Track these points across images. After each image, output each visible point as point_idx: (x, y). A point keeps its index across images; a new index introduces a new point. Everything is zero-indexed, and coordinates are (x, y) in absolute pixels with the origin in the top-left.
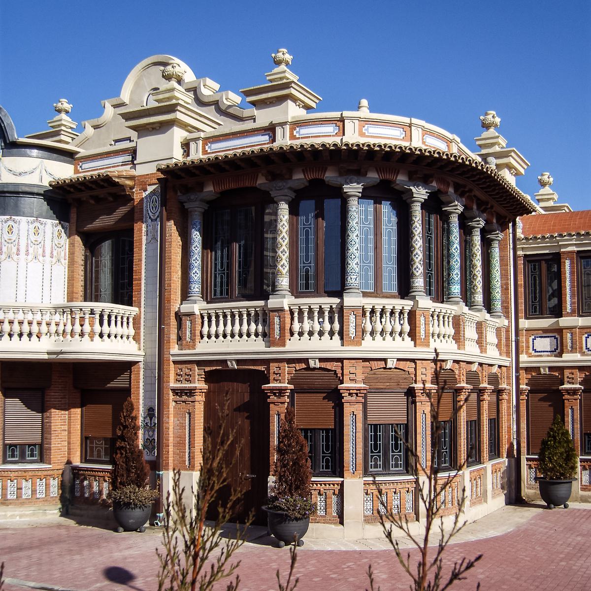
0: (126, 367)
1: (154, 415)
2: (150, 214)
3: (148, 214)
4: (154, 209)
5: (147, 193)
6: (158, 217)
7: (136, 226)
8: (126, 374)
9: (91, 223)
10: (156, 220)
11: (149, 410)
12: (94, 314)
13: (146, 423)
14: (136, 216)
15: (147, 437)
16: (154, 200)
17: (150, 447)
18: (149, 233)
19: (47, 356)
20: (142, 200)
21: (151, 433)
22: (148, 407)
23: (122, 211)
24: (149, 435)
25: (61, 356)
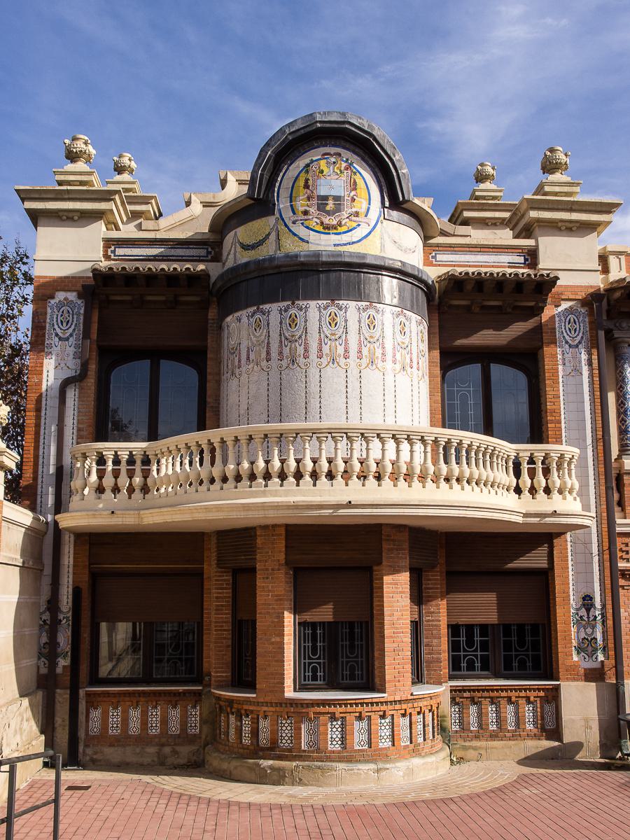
0: (543, 537)
1: (593, 605)
2: (567, 337)
3: (564, 337)
4: (573, 332)
5: (560, 309)
6: (580, 342)
7: (547, 350)
8: (543, 550)
9: (467, 336)
10: (577, 346)
11: (584, 599)
12: (534, 463)
13: (581, 617)
14: (545, 337)
15: (583, 635)
16: (572, 320)
17: (590, 649)
18: (566, 361)
19: (521, 518)
20: (553, 317)
21: (589, 630)
22: (582, 595)
23: (518, 329)
24: (586, 634)
25: (548, 520)
